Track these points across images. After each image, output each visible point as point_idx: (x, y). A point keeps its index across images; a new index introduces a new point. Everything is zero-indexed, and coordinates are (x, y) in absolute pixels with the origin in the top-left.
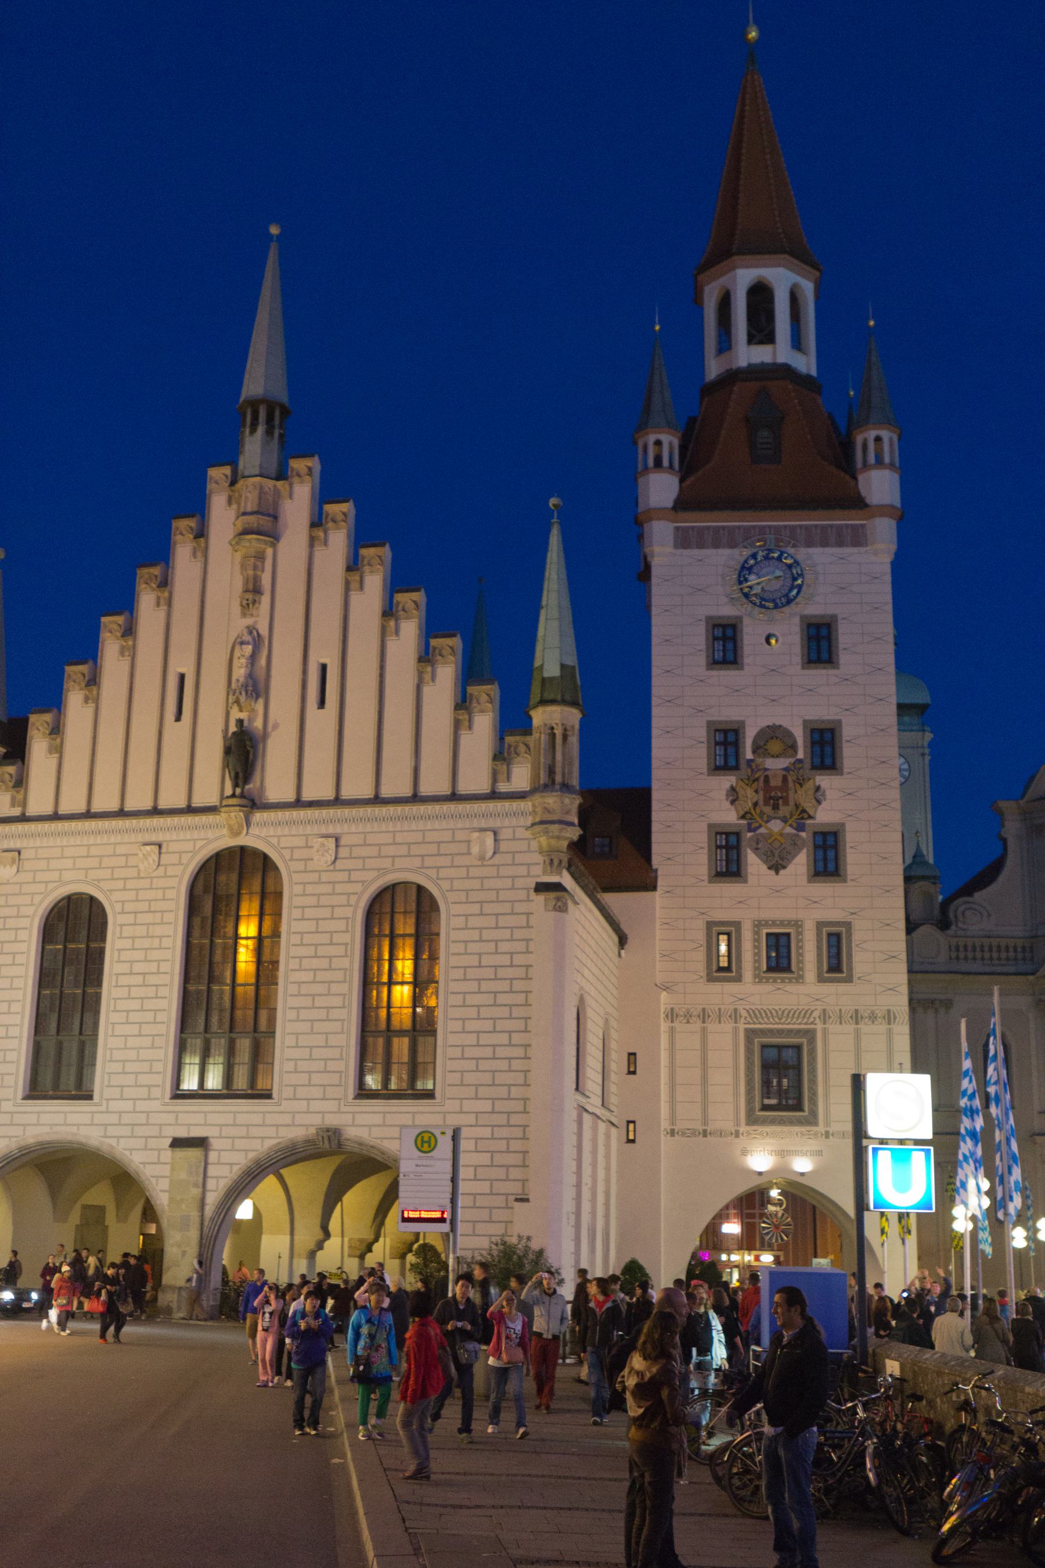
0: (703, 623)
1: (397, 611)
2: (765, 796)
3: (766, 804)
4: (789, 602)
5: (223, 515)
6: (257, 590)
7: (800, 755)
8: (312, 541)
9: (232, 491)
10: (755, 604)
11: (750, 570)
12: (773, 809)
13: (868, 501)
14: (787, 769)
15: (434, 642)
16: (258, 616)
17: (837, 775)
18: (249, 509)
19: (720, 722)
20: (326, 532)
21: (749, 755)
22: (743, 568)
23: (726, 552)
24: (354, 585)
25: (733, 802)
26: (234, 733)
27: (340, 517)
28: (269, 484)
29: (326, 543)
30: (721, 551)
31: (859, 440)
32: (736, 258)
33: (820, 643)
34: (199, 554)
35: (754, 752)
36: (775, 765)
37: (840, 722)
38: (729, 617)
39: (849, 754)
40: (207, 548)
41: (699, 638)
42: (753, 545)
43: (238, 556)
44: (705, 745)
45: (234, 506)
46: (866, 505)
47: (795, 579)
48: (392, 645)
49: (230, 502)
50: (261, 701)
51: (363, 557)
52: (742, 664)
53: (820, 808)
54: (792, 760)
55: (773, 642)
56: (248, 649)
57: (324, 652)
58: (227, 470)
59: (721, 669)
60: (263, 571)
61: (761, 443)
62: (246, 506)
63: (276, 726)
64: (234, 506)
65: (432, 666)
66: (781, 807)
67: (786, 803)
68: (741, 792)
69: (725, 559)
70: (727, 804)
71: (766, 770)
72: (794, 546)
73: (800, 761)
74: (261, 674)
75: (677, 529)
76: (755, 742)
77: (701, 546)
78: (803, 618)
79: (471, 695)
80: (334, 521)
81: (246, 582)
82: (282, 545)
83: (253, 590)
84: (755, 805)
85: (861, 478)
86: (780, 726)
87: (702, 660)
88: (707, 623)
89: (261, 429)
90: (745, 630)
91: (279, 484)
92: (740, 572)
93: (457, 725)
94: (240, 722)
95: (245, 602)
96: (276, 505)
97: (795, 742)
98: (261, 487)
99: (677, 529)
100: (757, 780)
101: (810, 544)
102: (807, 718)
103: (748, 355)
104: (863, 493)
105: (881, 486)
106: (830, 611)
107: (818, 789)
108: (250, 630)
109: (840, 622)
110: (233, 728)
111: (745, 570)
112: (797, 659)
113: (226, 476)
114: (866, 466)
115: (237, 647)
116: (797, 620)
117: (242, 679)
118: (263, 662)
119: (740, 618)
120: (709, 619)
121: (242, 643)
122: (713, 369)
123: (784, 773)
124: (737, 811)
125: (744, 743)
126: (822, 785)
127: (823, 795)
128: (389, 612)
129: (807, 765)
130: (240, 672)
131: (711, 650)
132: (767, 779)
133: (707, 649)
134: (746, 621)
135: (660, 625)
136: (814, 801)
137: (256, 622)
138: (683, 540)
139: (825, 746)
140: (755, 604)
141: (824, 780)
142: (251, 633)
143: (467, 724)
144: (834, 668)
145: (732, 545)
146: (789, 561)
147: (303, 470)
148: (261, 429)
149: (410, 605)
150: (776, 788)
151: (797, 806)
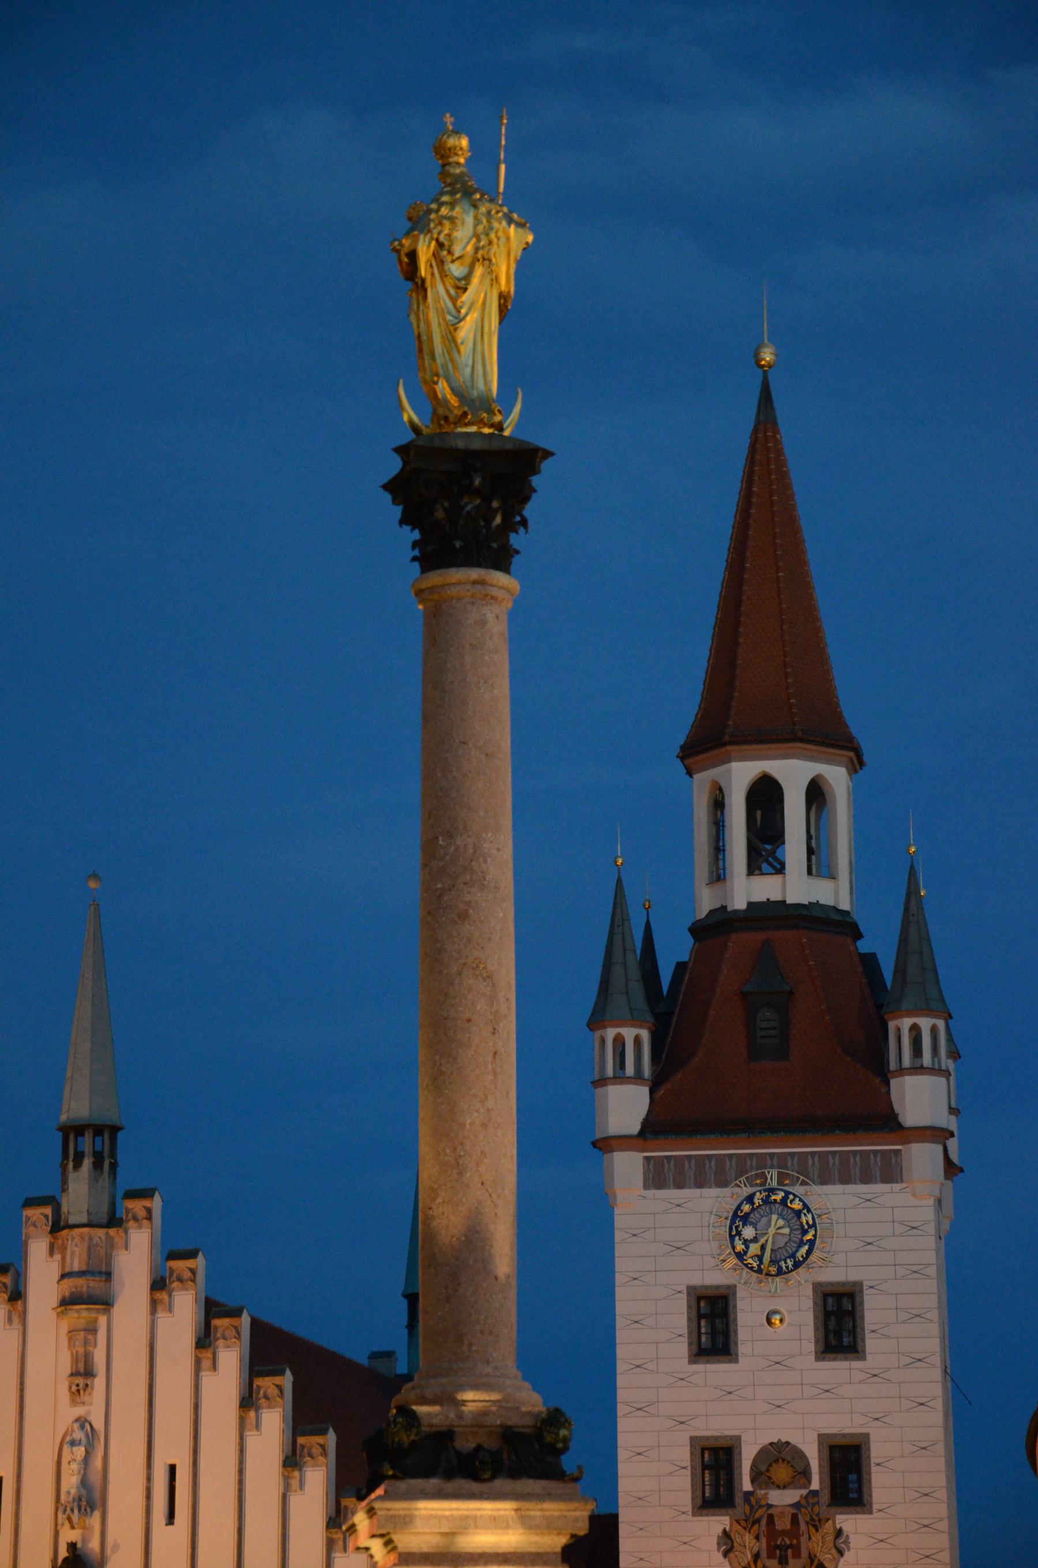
0: (684, 1296)
1: (258, 1399)
2: (768, 1545)
3: (771, 1555)
4: (797, 1265)
5: (43, 1273)
6: (89, 1373)
7: (815, 1485)
8: (154, 1305)
9: (54, 1238)
10: (751, 1269)
11: (745, 1219)
12: (780, 1563)
13: (901, 1119)
14: (797, 1505)
15: (301, 1440)
16: (91, 1404)
17: (864, 1513)
18: (76, 1269)
19: (707, 1438)
20: (170, 1296)
21: (747, 1486)
22: (735, 1215)
23: (715, 1191)
24: (206, 1363)
25: (726, 1554)
26: (65, 1560)
27: (187, 1275)
28: (100, 1233)
29: (170, 1310)
30: (706, 1191)
31: (892, 1025)
32: (730, 748)
33: (840, 1323)
34: (16, 1319)
35: (753, 1481)
36: (782, 1498)
37: (867, 1436)
38: (718, 1287)
39: (882, 1483)
40: (24, 1312)
41: (678, 1317)
42: (750, 1182)
43: (64, 1326)
44: (688, 1472)
45: (58, 1257)
46: (900, 1126)
47: (805, 1232)
48: (252, 1441)
49: (51, 1253)
50: (97, 1515)
51: (216, 1328)
52: (737, 1355)
53: (842, 1560)
54: (804, 1492)
55: (777, 1320)
56: (80, 1451)
57: (173, 1448)
58: (48, 1211)
59: (708, 1362)
60: (95, 1345)
61: (761, 1029)
62: (72, 1264)
63: (116, 1547)
64: (58, 1257)
65: (300, 1470)
66: (790, 1560)
67: (797, 1555)
68: (737, 1539)
69: (715, 1201)
70: (719, 1557)
71: (770, 1506)
72: (804, 1183)
73: (815, 1493)
74: (95, 1478)
75: (647, 1159)
76: (754, 1466)
77: (680, 1186)
78: (817, 1286)
79: (346, 1508)
80: (180, 1280)
81: (75, 1360)
82: (117, 1310)
83: (83, 1373)
84: (756, 1557)
85: (893, 1082)
86: (788, 1443)
87: (682, 1348)
88: (688, 1294)
89: (87, 1163)
90: (740, 1305)
91: (112, 1231)
92: (733, 1222)
93: (330, 1545)
94: (72, 1546)
95: (74, 1388)
96: (109, 1259)
97: (808, 1464)
98: (91, 1239)
99: (647, 1159)
100: (758, 1521)
101: (825, 1180)
102: (823, 1431)
103: (745, 890)
104: (897, 1108)
105: (918, 1098)
106: (853, 1276)
107: (839, 1533)
108: (82, 1422)
109: (865, 1292)
110: (63, 1553)
111: (739, 1218)
112: (810, 1347)
113: (46, 1217)
114: (901, 1071)
115: (66, 1448)
116: (809, 1291)
117: (73, 1491)
118: (98, 1462)
119: (732, 1288)
120: (691, 1290)
121: (73, 1443)
122: (706, 902)
123: (793, 1511)
124: (731, 1564)
125: (740, 1467)
126: (844, 1529)
127: (847, 1542)
128: (248, 1401)
129: (825, 1497)
130: (71, 1482)
131: (695, 1334)
132: (771, 1519)
133: (690, 1333)
134: (740, 1293)
135: (628, 1301)
136: (834, 1551)
137: (89, 1412)
138: (657, 1177)
139: (847, 1468)
140: (751, 1269)
141: (847, 1521)
142: (82, 1427)
143: (341, 1543)
144: (859, 1359)
145: (722, 1184)
146: (797, 1205)
147: (142, 1214)
148: (87, 1163)
149: (273, 1391)
150: (783, 1533)
151: (812, 1558)
